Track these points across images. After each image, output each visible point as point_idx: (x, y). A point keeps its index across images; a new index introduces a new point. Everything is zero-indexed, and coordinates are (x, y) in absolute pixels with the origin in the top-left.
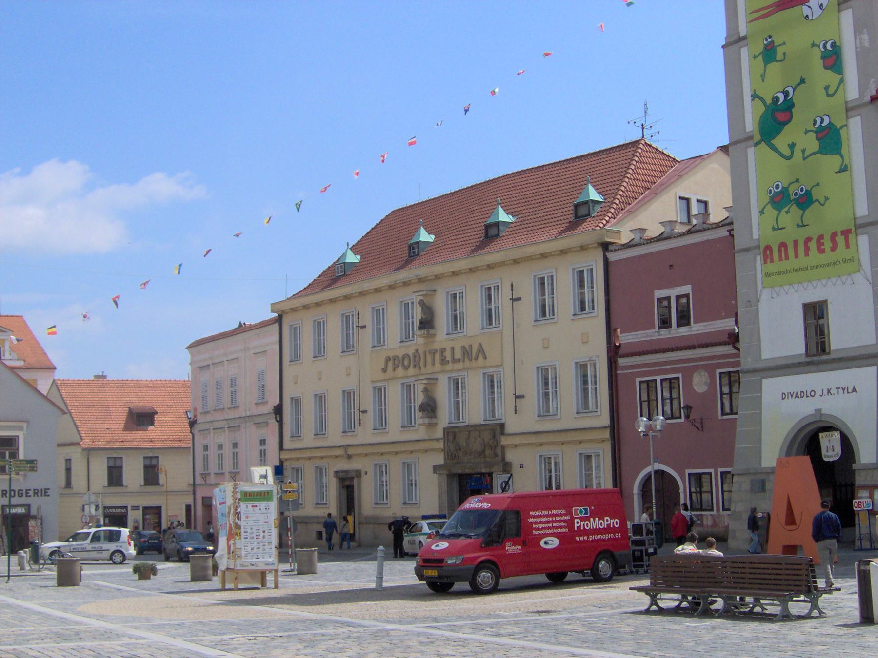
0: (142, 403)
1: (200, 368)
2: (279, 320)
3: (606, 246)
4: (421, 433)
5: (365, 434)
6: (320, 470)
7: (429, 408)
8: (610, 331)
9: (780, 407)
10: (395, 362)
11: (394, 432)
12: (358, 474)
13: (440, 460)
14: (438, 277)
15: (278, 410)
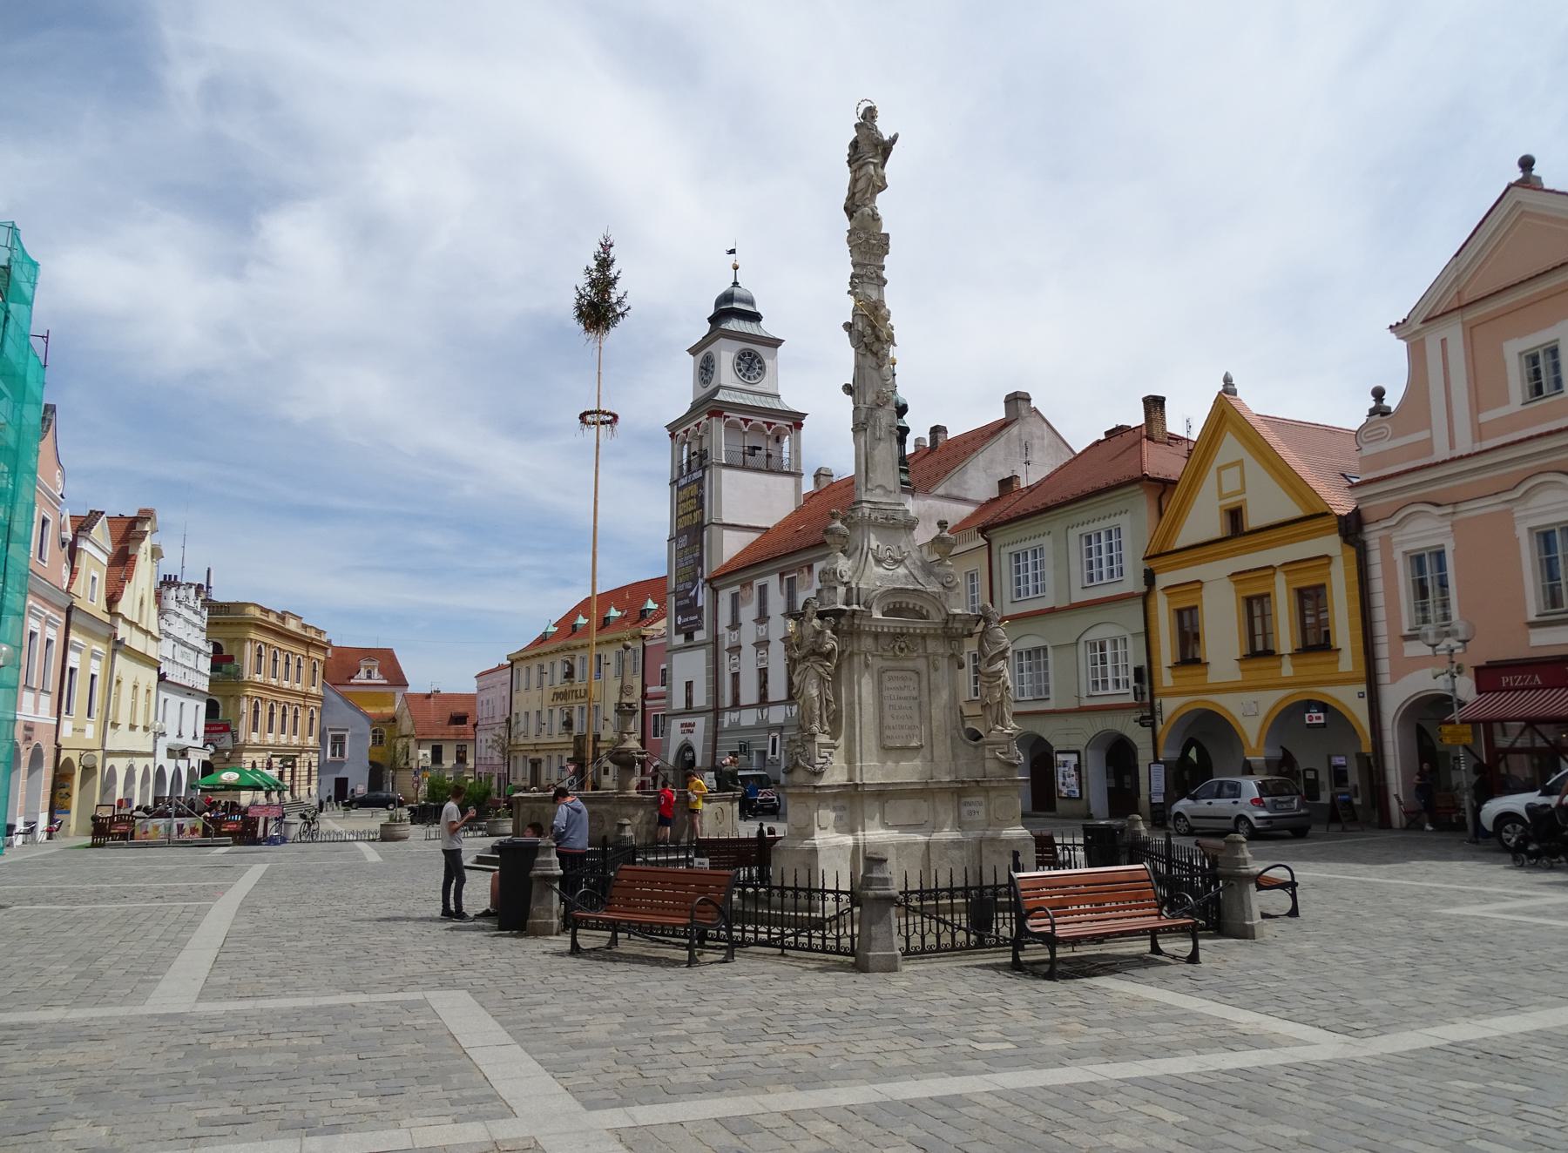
0: (461, 710)
1: (480, 690)
2: (511, 666)
3: (644, 637)
4: (565, 739)
5: (544, 739)
6: (561, 757)
7: (568, 724)
8: (644, 686)
9: (676, 735)
10: (558, 695)
11: (556, 739)
12: (540, 761)
13: (571, 755)
14: (576, 648)
15: (509, 721)
